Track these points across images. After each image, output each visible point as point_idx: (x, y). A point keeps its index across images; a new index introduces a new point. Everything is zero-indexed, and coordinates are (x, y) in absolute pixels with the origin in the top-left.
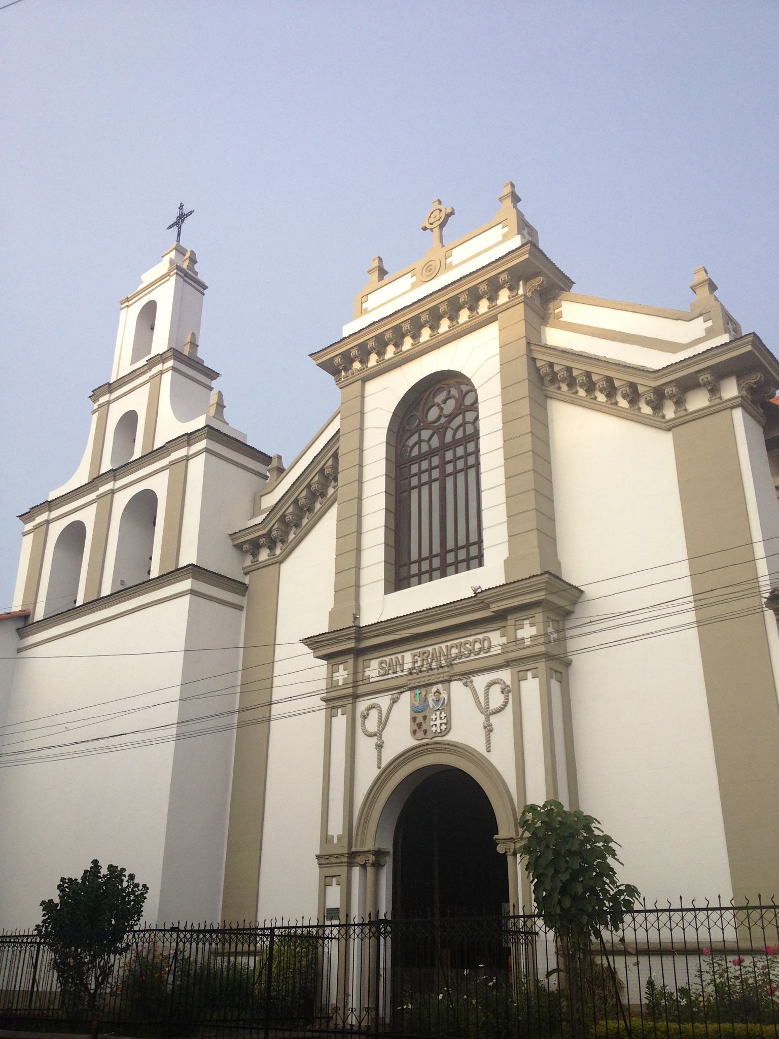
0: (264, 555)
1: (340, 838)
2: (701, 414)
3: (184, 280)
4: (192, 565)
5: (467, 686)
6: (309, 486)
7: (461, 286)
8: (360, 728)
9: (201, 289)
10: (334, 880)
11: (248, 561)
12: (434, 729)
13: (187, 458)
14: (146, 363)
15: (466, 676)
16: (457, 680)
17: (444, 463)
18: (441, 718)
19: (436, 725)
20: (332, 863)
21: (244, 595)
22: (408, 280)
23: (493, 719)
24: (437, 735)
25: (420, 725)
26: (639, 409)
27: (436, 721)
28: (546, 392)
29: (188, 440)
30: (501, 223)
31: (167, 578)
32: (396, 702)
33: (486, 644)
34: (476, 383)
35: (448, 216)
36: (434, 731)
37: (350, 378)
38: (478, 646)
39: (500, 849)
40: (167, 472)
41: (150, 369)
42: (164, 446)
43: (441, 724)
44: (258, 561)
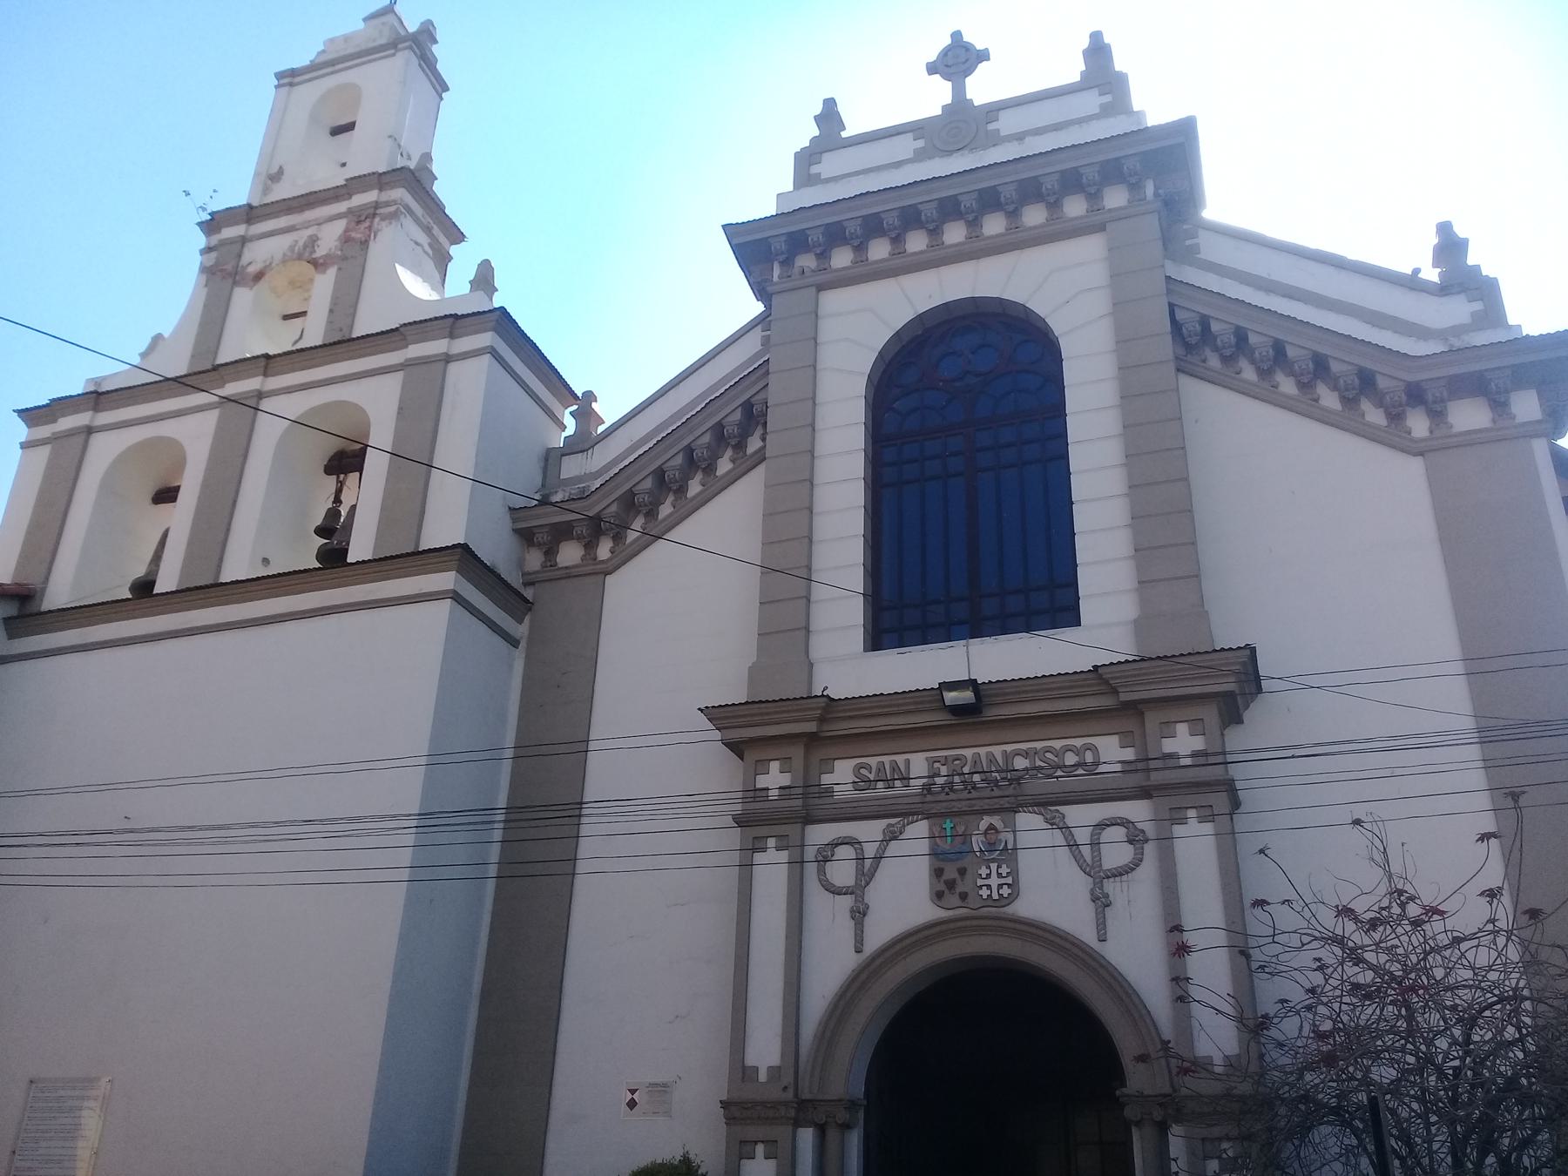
0: (570, 554)
2: (1472, 440)
3: (420, 65)
4: (464, 548)
5: (1052, 824)
8: (815, 876)
9: (440, 90)
10: (760, 1149)
11: (535, 559)
12: (985, 893)
13: (448, 359)
14: (345, 183)
18: (999, 875)
19: (989, 887)
21: (520, 621)
23: (1111, 887)
24: (990, 903)
25: (951, 885)
26: (1363, 415)
27: (990, 880)
28: (1182, 363)
29: (452, 327)
31: (385, 565)
32: (895, 838)
33: (1089, 757)
34: (1057, 325)
36: (985, 897)
38: (1071, 759)
39: (1128, 1112)
40: (399, 376)
41: (350, 196)
42: (397, 329)
43: (1000, 886)
44: (556, 564)
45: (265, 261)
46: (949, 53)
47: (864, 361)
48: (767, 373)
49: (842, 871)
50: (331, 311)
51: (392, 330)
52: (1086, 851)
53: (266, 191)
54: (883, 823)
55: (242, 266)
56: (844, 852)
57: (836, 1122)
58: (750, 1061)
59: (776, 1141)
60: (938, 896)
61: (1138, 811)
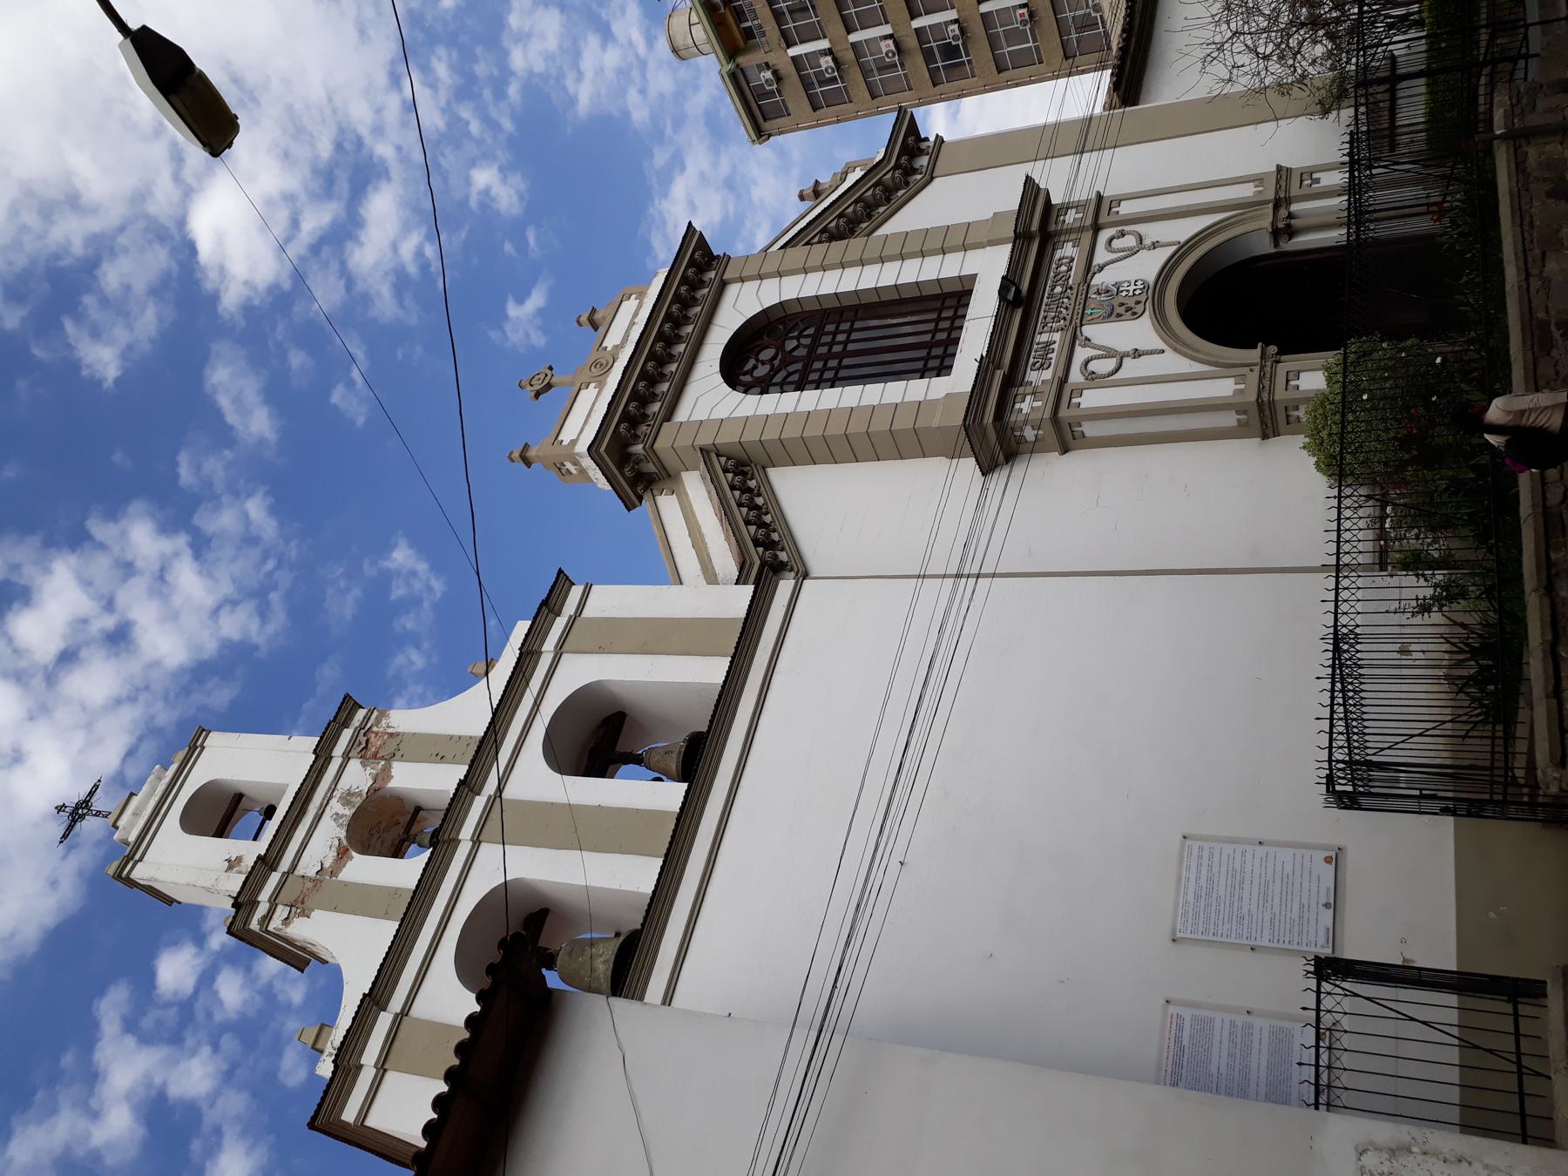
1: (1240, 378)
6: (740, 505)
7: (671, 285)
14: (314, 756)
15: (1089, 269)
16: (1093, 276)
17: (826, 358)
19: (1135, 290)
20: (1271, 381)
22: (587, 396)
23: (1147, 242)
29: (550, 611)
30: (621, 301)
32: (1089, 340)
35: (551, 368)
37: (650, 433)
38: (1064, 268)
41: (329, 759)
42: (521, 654)
43: (1135, 285)
45: (331, 847)
46: (532, 383)
47: (738, 396)
48: (708, 452)
49: (1103, 366)
50: (443, 757)
51: (519, 659)
52: (1119, 255)
53: (241, 873)
54: (1078, 349)
55: (317, 873)
56: (1092, 366)
57: (1276, 354)
58: (1230, 393)
59: (1287, 372)
60: (1135, 313)
61: (1104, 236)
